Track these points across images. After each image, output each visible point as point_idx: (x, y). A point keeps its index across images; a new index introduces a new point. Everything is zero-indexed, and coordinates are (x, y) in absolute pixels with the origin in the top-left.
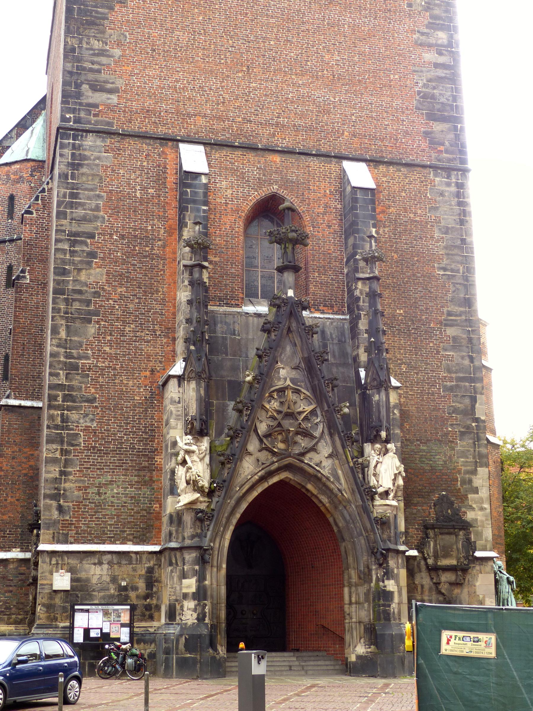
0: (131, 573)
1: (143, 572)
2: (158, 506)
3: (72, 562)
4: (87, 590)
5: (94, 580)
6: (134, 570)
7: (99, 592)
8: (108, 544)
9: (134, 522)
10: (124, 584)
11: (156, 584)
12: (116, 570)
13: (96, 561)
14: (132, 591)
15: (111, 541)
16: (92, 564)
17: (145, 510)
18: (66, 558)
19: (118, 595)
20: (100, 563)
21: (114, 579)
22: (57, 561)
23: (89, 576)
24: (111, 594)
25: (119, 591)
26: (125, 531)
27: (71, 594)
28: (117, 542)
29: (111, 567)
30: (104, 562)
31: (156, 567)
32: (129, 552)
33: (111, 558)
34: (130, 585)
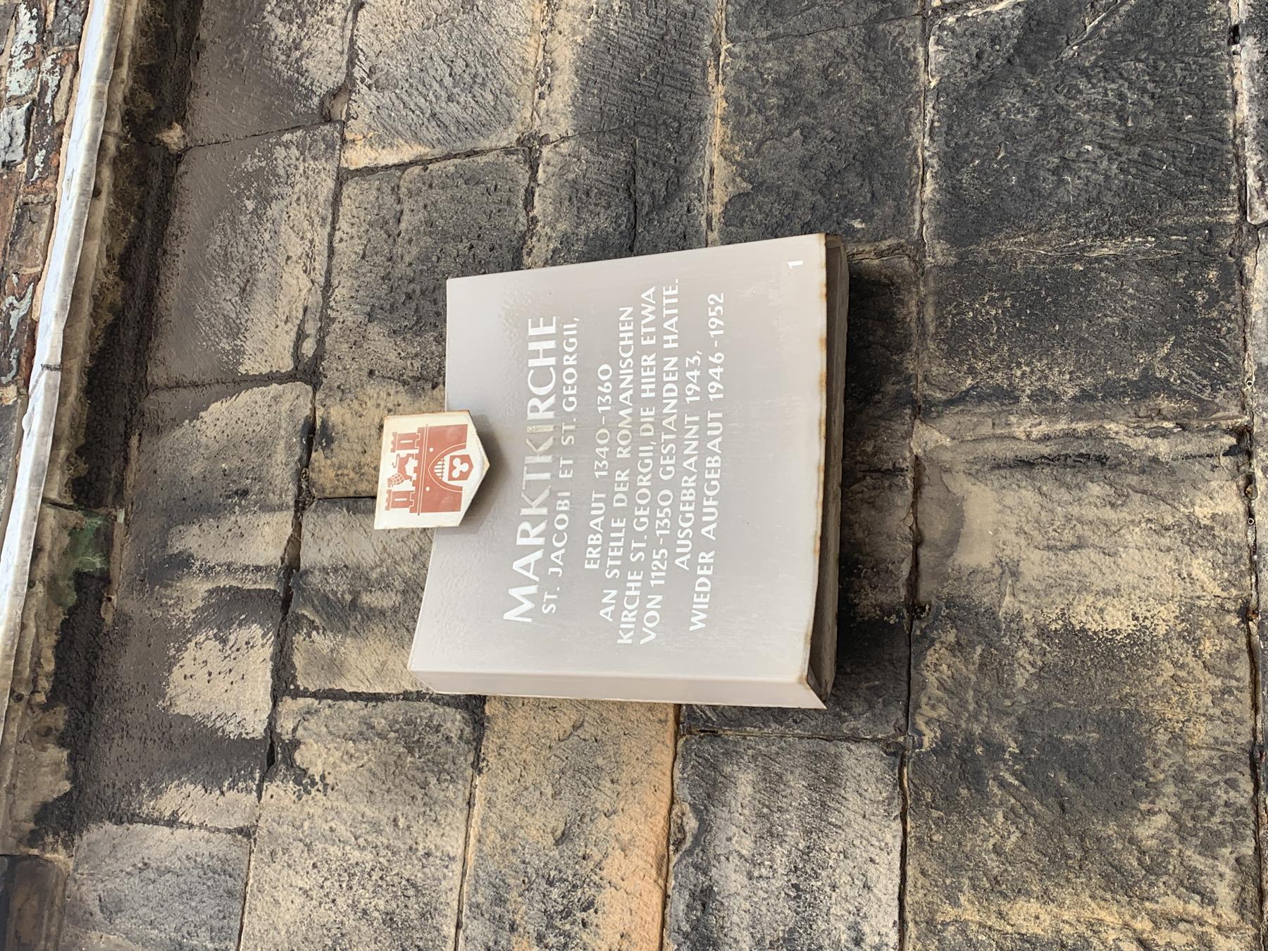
3: (298, 287)
18: (221, 418)
22: (230, 607)
27: (966, 218)
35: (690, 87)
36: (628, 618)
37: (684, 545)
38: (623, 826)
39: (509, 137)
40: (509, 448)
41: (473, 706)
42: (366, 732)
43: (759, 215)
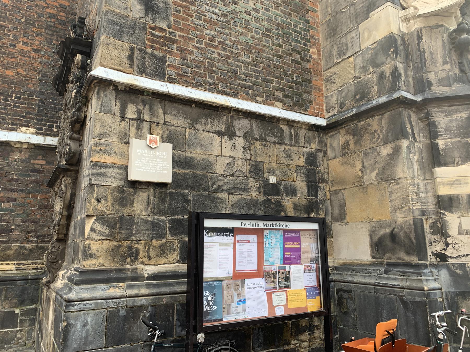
0: (284, 161)
1: (302, 162)
2: (315, 51)
3: (174, 122)
4: (207, 188)
5: (220, 167)
6: (289, 156)
7: (229, 192)
8: (242, 98)
9: (282, 68)
10: (272, 180)
11: (321, 185)
12: (259, 152)
13: (223, 128)
14: (287, 195)
15: (248, 94)
16: (215, 133)
17: (299, 53)
18: (161, 111)
19: (264, 202)
20: (230, 134)
21: (256, 170)
22: (139, 112)
23: (211, 158)
24: (251, 200)
25: (265, 194)
26: (269, 82)
27: (171, 194)
28: (259, 99)
29: (251, 144)
30: (238, 133)
31: (320, 155)
32: (278, 120)
33: (249, 126)
34: (283, 184)
35: (188, 168)
36: (137, 162)
37: (144, 168)
38: (116, 159)
39: (187, 149)
40: (155, 149)
41: (128, 143)
42: (126, 130)
43: (174, 175)
